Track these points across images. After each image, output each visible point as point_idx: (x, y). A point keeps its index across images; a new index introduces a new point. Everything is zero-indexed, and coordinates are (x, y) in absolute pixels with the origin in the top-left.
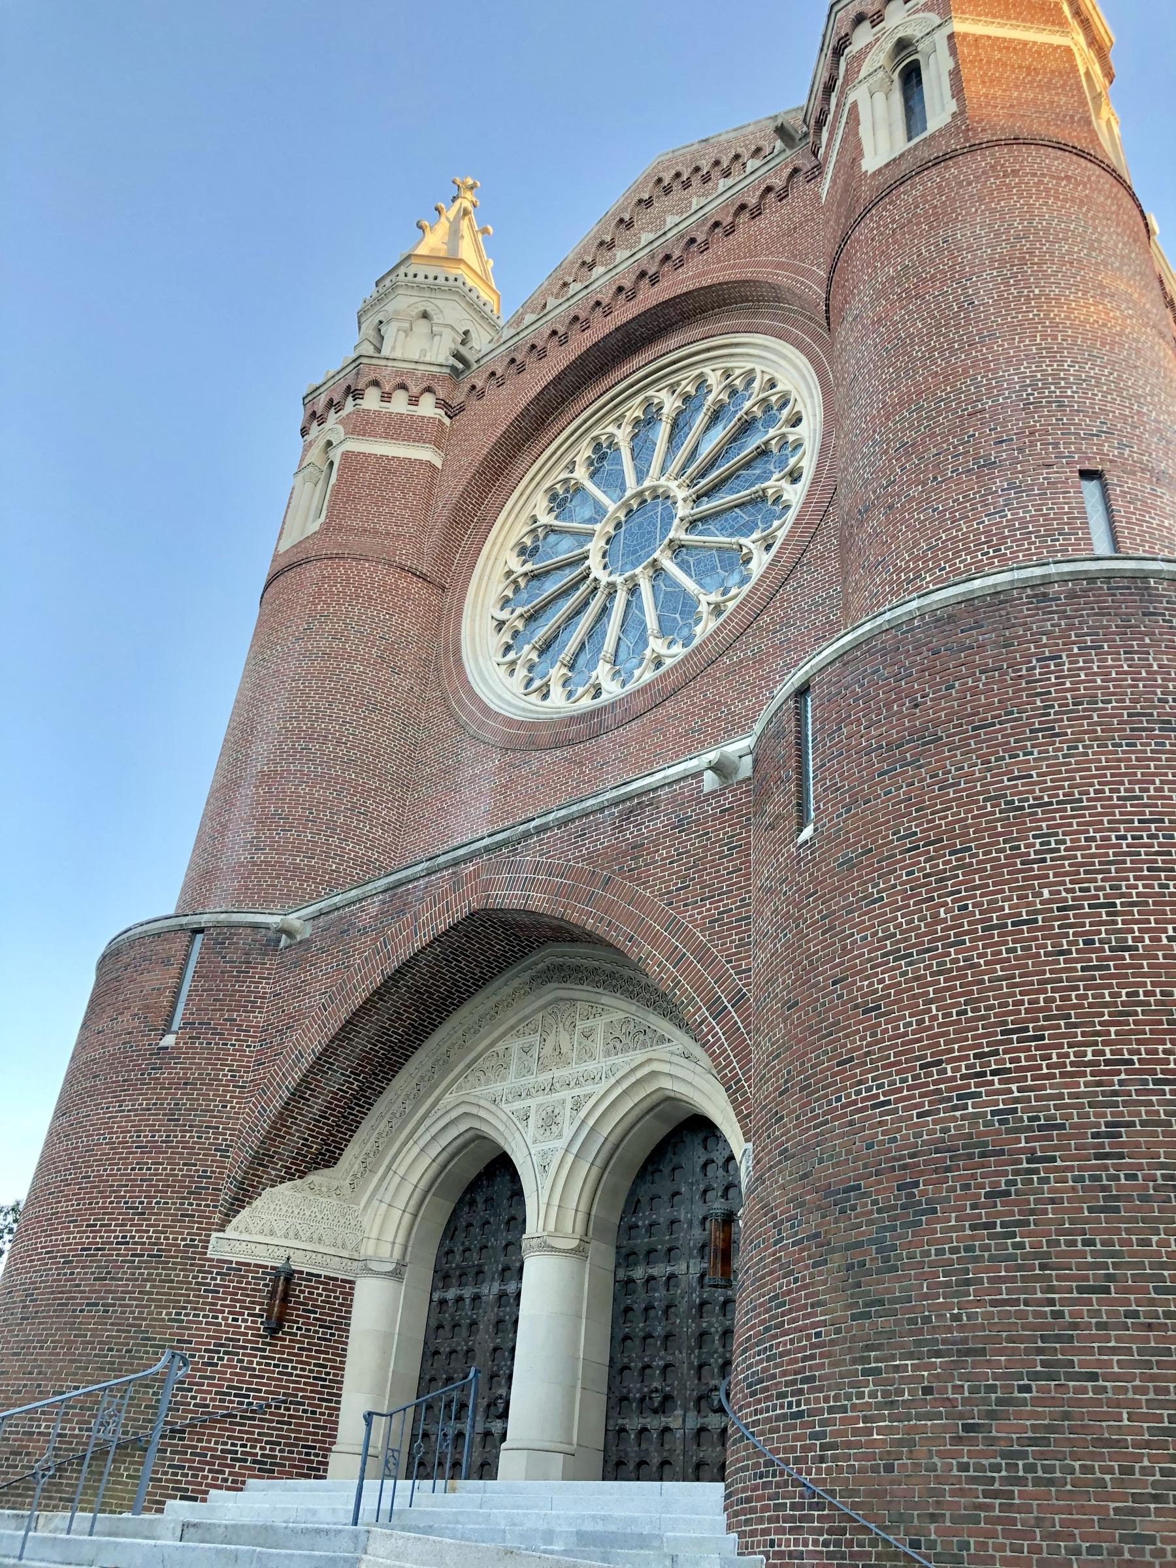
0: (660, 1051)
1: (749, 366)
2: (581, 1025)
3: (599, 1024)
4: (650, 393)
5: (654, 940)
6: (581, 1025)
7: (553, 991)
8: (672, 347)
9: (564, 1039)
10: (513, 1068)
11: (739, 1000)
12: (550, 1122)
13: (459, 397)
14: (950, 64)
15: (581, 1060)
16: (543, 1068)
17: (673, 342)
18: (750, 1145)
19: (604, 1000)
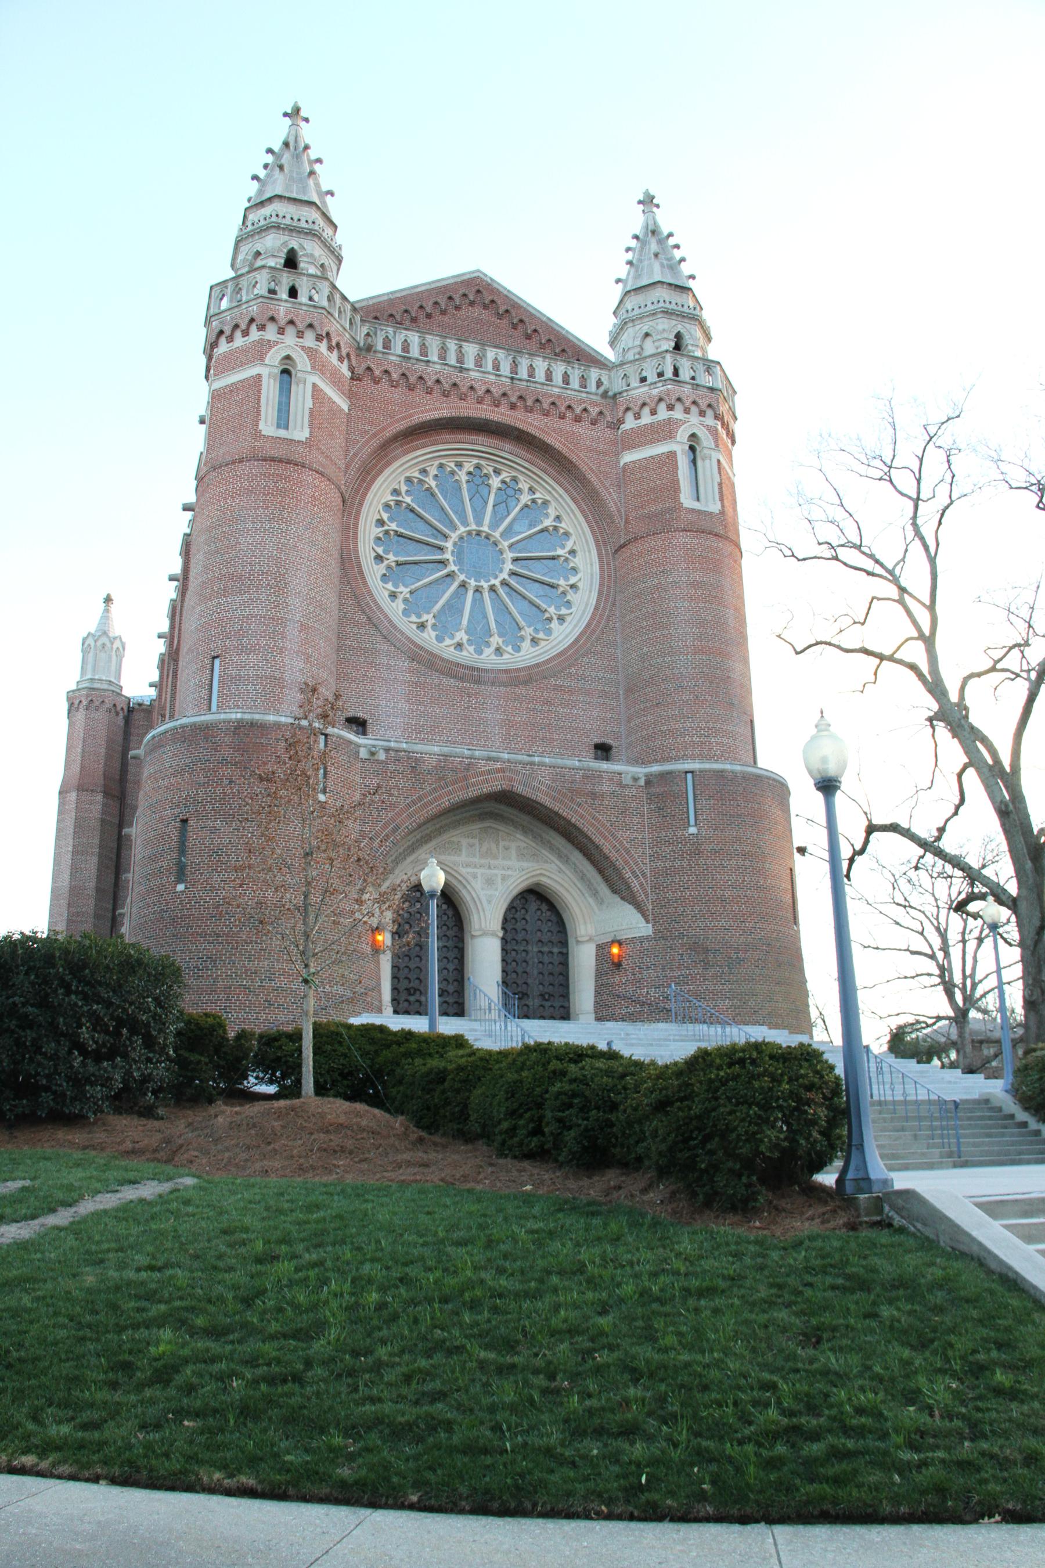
0: (546, 866)
1: (548, 498)
2: (502, 844)
3: (513, 845)
4: (483, 462)
5: (605, 838)
6: (502, 844)
7: (487, 824)
8: (507, 449)
9: (493, 846)
10: (464, 852)
11: (644, 875)
12: (489, 882)
13: (360, 371)
14: (717, 479)
15: (504, 858)
16: (482, 856)
17: (508, 446)
18: (650, 925)
19: (518, 836)
